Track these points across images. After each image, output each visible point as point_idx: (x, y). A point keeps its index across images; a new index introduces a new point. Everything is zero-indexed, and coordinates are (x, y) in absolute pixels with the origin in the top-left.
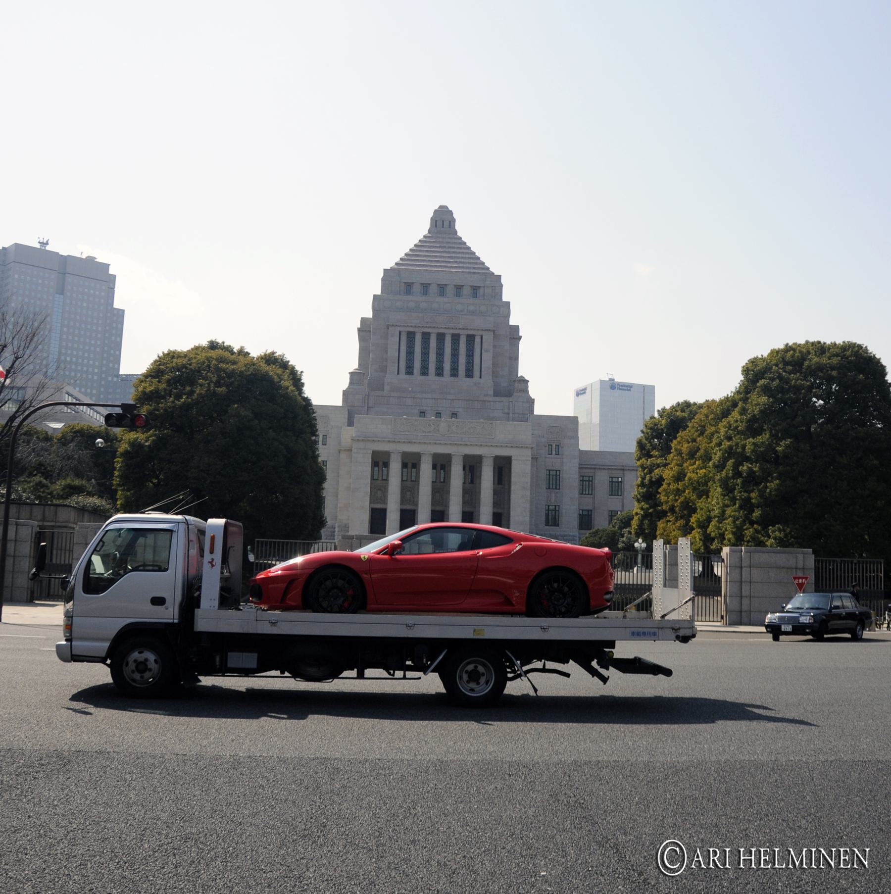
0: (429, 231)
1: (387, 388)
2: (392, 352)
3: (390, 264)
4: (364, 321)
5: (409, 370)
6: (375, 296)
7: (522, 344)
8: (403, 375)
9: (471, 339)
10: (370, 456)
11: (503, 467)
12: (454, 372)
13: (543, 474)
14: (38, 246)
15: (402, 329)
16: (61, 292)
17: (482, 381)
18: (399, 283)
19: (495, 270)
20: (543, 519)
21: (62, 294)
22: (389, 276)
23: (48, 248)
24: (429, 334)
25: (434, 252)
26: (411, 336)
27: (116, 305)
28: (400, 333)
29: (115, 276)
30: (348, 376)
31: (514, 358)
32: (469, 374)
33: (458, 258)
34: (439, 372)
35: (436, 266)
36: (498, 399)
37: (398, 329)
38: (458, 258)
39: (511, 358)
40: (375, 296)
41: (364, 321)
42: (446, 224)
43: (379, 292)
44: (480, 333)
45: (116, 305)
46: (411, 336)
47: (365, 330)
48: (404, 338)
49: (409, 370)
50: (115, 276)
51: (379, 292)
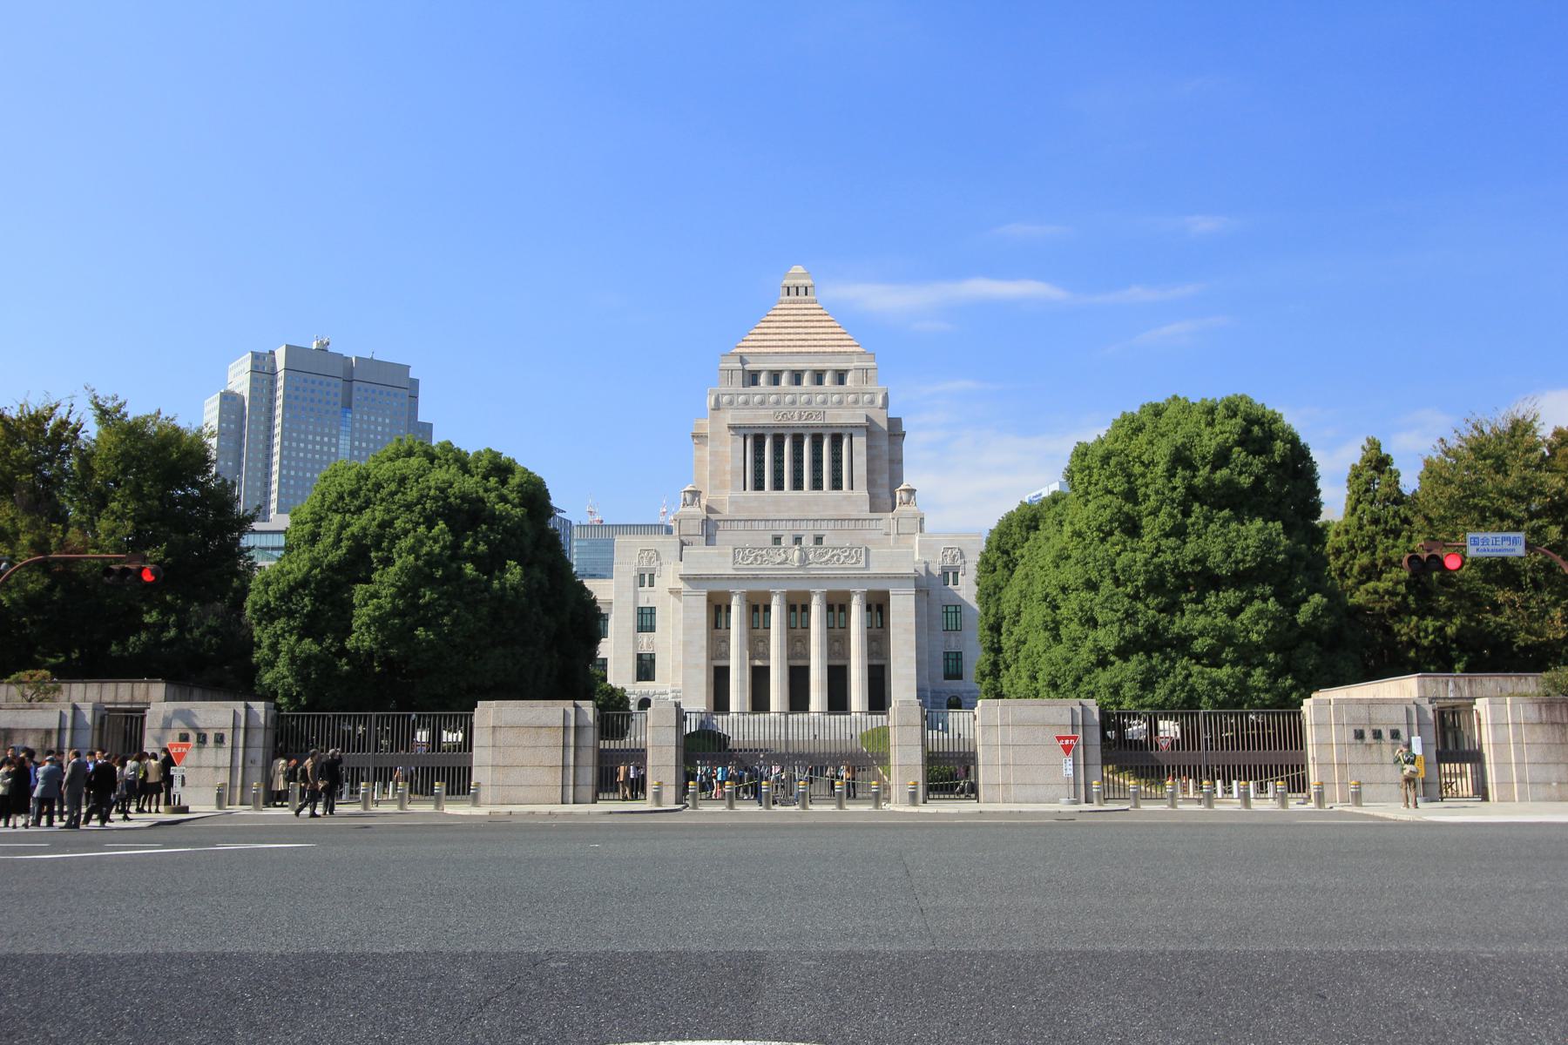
5: (759, 485)
7: (907, 445)
8: (750, 493)
9: (837, 440)
10: (704, 599)
11: (878, 607)
12: (817, 484)
13: (938, 611)
17: (855, 492)
20: (941, 671)
26: (759, 441)
27: (422, 417)
31: (896, 463)
32: (837, 484)
34: (797, 485)
36: (875, 515)
37: (743, 431)
39: (891, 461)
42: (802, 291)
44: (849, 431)
45: (422, 417)
46: (759, 441)
49: (759, 485)
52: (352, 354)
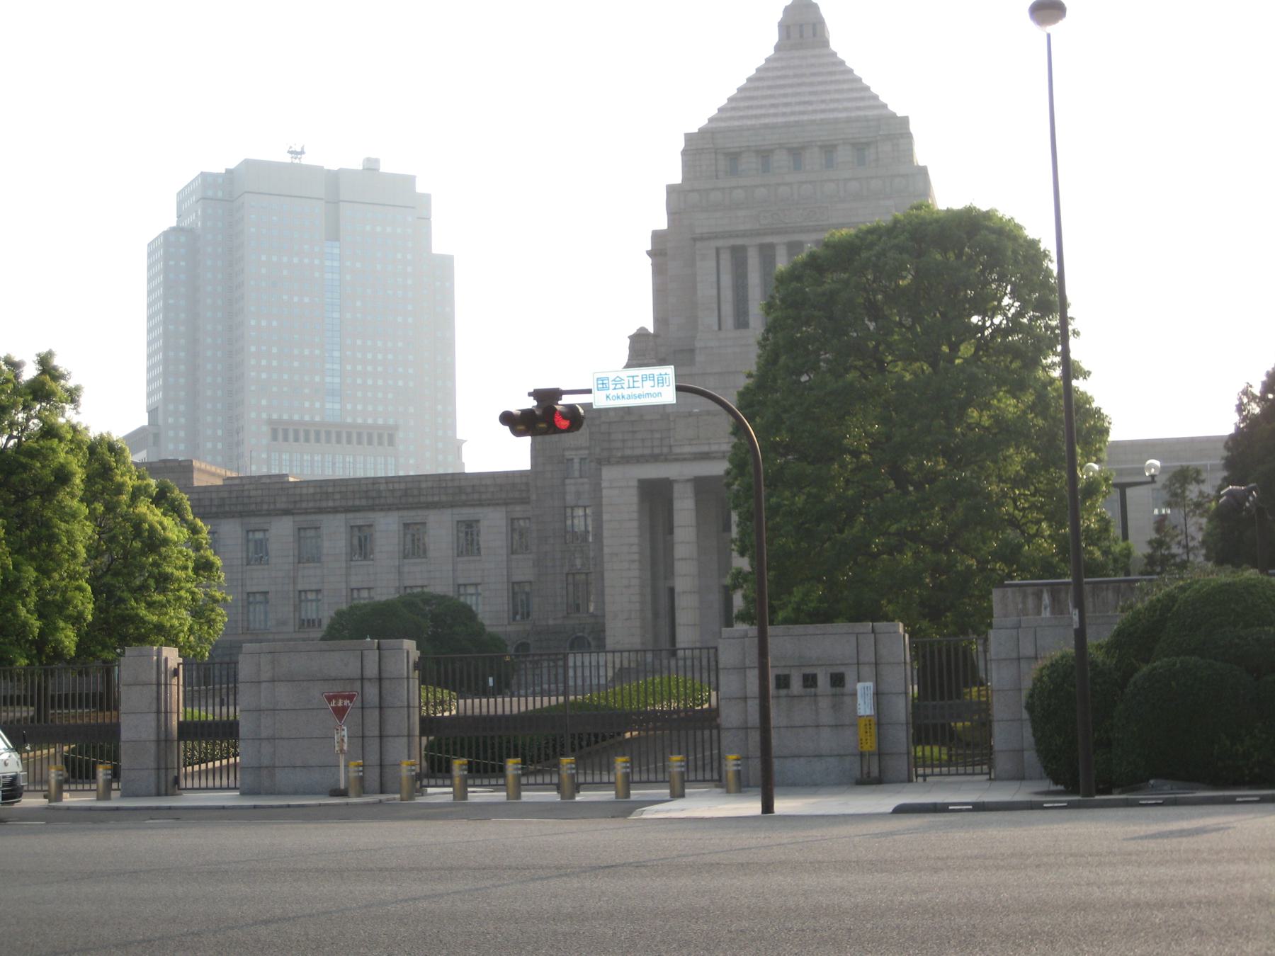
0: (778, 48)
1: (699, 358)
2: (706, 291)
3: (696, 122)
4: (657, 236)
6: (671, 190)
14: (287, 159)
15: (720, 243)
16: (334, 234)
18: (716, 155)
19: (898, 107)
21: (337, 239)
22: (699, 149)
23: (306, 160)
24: (772, 247)
25: (783, 86)
26: (739, 255)
28: (718, 250)
29: (428, 197)
30: (628, 341)
33: (828, 92)
35: (784, 114)
38: (828, 92)
40: (671, 190)
41: (657, 236)
43: (677, 178)
46: (739, 255)
47: (661, 249)
48: (726, 259)
50: (428, 197)
51: (677, 178)
52: (332, 164)
